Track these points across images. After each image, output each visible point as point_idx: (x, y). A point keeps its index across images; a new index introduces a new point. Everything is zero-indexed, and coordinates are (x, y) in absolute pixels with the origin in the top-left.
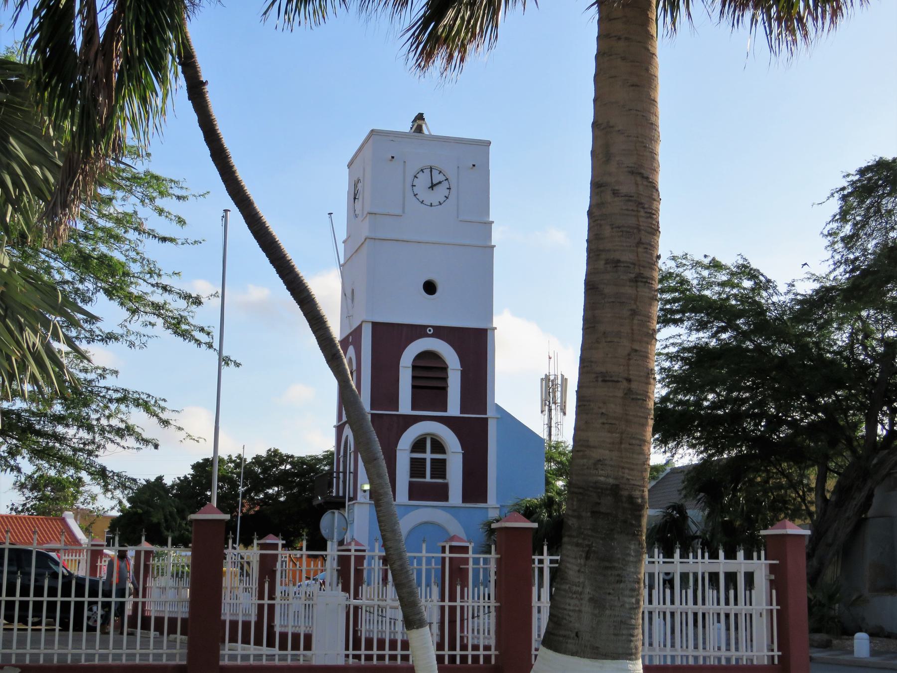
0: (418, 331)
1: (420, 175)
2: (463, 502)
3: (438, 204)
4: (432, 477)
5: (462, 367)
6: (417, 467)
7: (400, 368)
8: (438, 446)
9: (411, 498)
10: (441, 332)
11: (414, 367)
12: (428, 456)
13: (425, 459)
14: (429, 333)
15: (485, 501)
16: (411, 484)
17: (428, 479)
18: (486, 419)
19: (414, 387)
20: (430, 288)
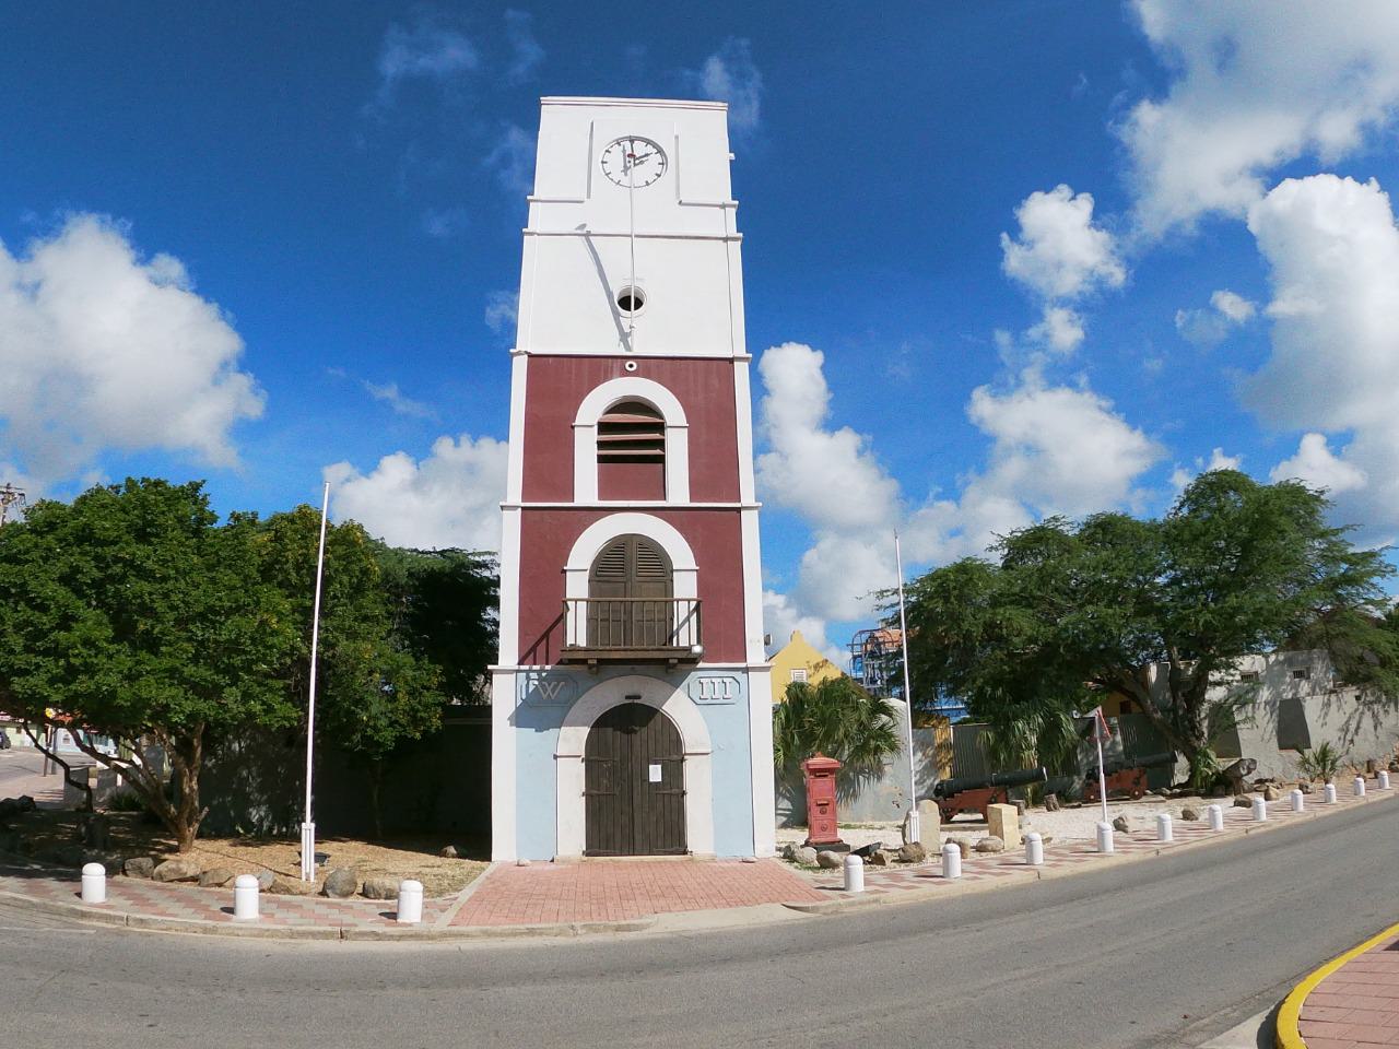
10: (651, 366)
11: (604, 427)
14: (632, 369)
18: (738, 510)
19: (602, 459)
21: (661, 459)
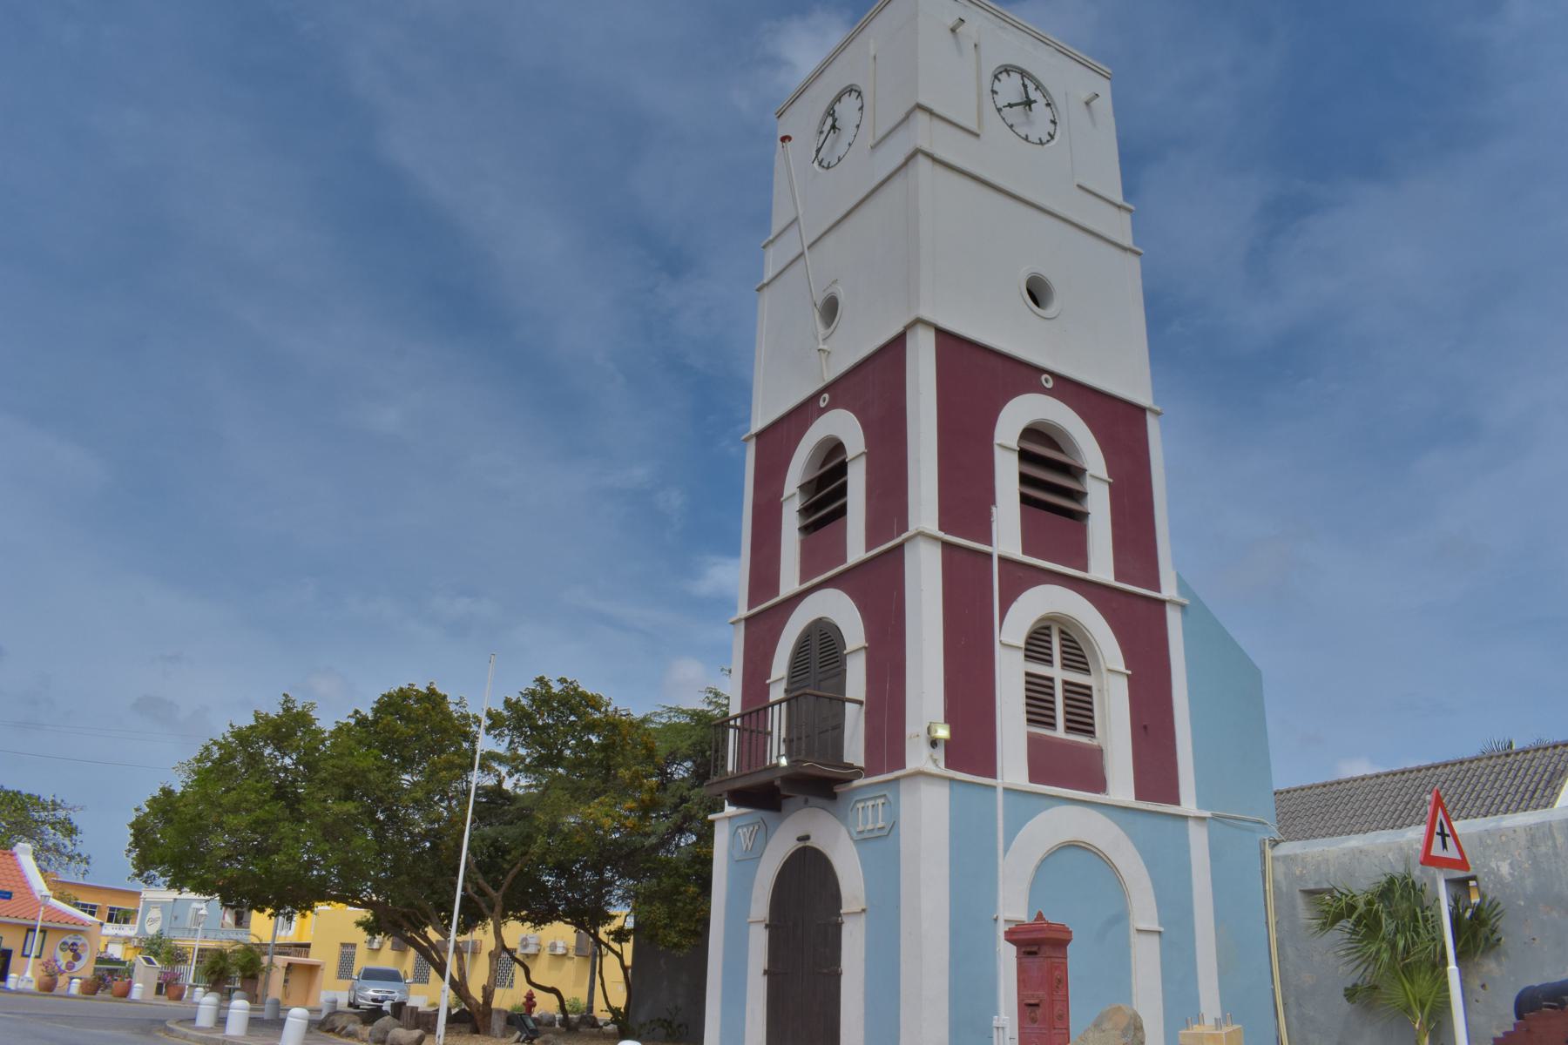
0: (1024, 376)
1: (1003, 77)
2: (1140, 796)
3: (1039, 142)
4: (1069, 729)
5: (1110, 472)
6: (1038, 697)
7: (997, 450)
8: (1077, 657)
9: (1034, 777)
10: (1070, 390)
11: (1025, 456)
12: (1057, 673)
13: (1051, 679)
15: (1175, 799)
16: (1034, 743)
17: (1060, 732)
18: (1162, 603)
19: (1025, 500)
20: (1037, 293)
21: (1081, 517)
